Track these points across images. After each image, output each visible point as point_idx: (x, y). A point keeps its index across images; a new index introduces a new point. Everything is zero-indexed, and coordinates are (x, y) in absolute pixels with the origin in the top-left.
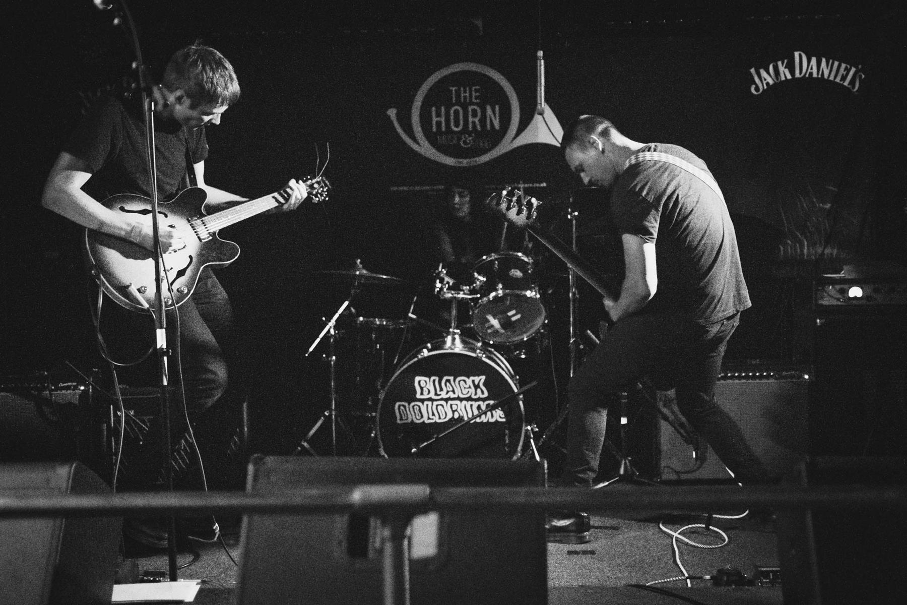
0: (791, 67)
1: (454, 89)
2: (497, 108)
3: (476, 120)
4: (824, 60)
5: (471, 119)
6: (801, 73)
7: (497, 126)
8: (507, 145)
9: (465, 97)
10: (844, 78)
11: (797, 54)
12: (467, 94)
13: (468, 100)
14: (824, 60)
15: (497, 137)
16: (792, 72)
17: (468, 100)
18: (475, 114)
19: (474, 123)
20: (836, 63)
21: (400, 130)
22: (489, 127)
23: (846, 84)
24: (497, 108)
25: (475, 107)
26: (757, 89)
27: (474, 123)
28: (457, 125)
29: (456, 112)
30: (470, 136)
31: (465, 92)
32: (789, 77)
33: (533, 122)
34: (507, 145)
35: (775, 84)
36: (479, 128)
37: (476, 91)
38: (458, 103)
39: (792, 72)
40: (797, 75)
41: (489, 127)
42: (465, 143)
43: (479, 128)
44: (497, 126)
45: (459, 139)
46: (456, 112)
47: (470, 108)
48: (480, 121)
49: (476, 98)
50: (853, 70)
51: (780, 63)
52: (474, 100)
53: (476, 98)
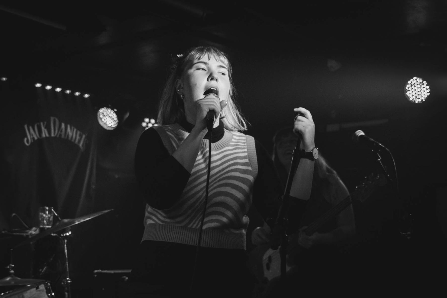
0: (48, 128)
4: (69, 126)
6: (54, 134)
10: (79, 142)
11: (52, 119)
14: (69, 126)
16: (49, 132)
20: (75, 130)
23: (81, 145)
26: (28, 141)
32: (47, 135)
35: (38, 139)
39: (49, 132)
40: (52, 135)
50: (84, 136)
51: (42, 124)
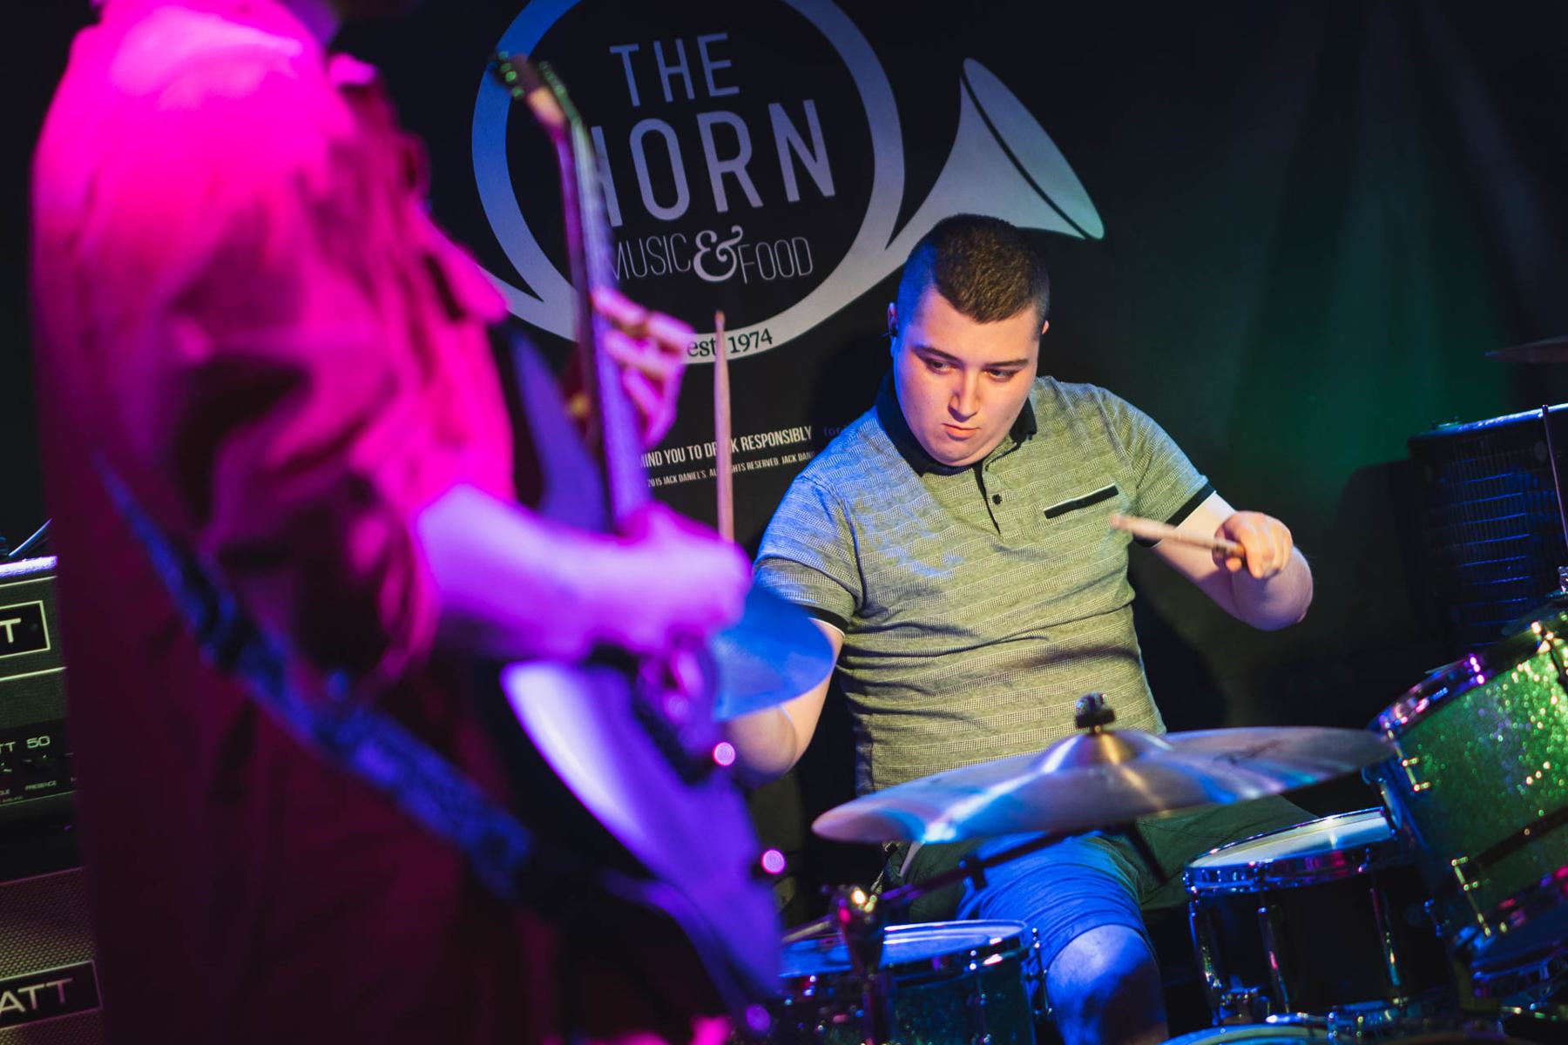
1: (625, 51)
2: (810, 107)
3: (738, 166)
5: (716, 169)
7: (828, 189)
9: (676, 81)
12: (683, 69)
13: (691, 95)
15: (830, 231)
17: (691, 95)
18: (727, 149)
19: (730, 180)
22: (793, 195)
24: (810, 107)
27: (730, 180)
28: (666, 197)
29: (654, 143)
30: (725, 235)
31: (672, 60)
36: (755, 201)
37: (715, 52)
38: (655, 106)
41: (793, 195)
42: (710, 264)
43: (755, 201)
44: (828, 189)
45: (687, 252)
46: (654, 143)
47: (705, 121)
48: (749, 168)
49: (721, 78)
52: (713, 92)
53: (721, 78)
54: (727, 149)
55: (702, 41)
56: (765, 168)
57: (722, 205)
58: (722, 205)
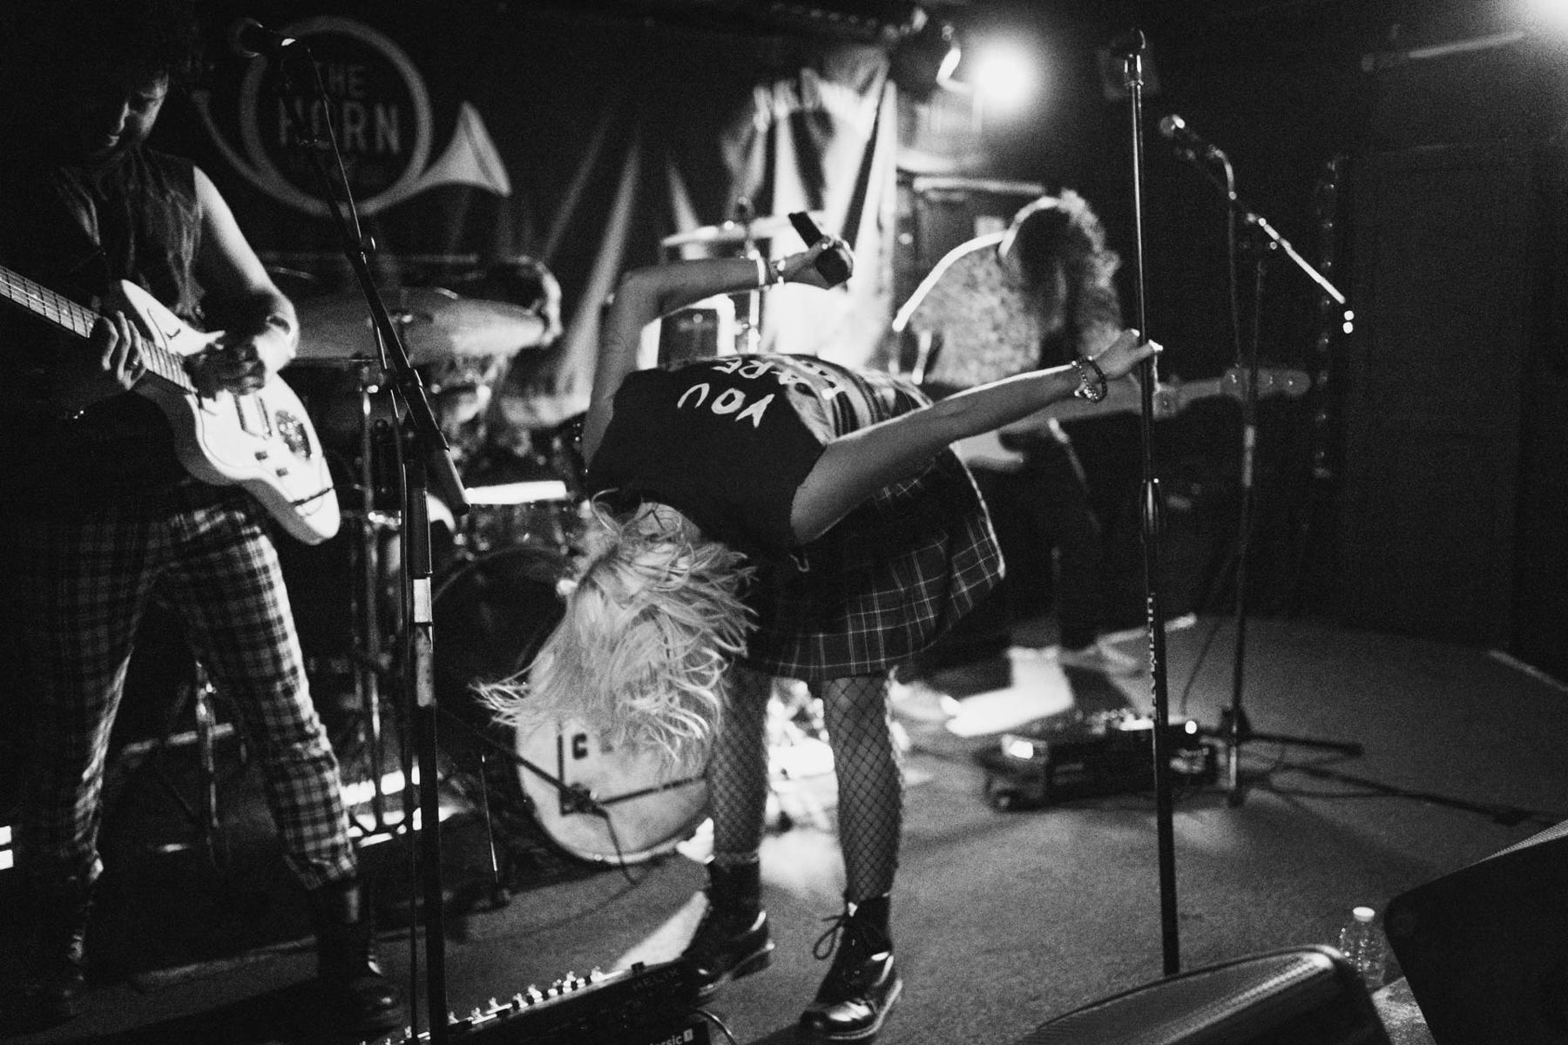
3: (359, 129)
5: (348, 129)
8: (415, 181)
15: (397, 165)
19: (354, 137)
21: (220, 142)
22: (380, 146)
24: (394, 112)
25: (355, 105)
27: (354, 137)
33: (456, 143)
34: (415, 181)
36: (362, 143)
47: (348, 107)
49: (358, 88)
53: (358, 88)
54: (354, 120)
55: (352, 69)
56: (370, 132)
57: (348, 145)
58: (348, 145)
